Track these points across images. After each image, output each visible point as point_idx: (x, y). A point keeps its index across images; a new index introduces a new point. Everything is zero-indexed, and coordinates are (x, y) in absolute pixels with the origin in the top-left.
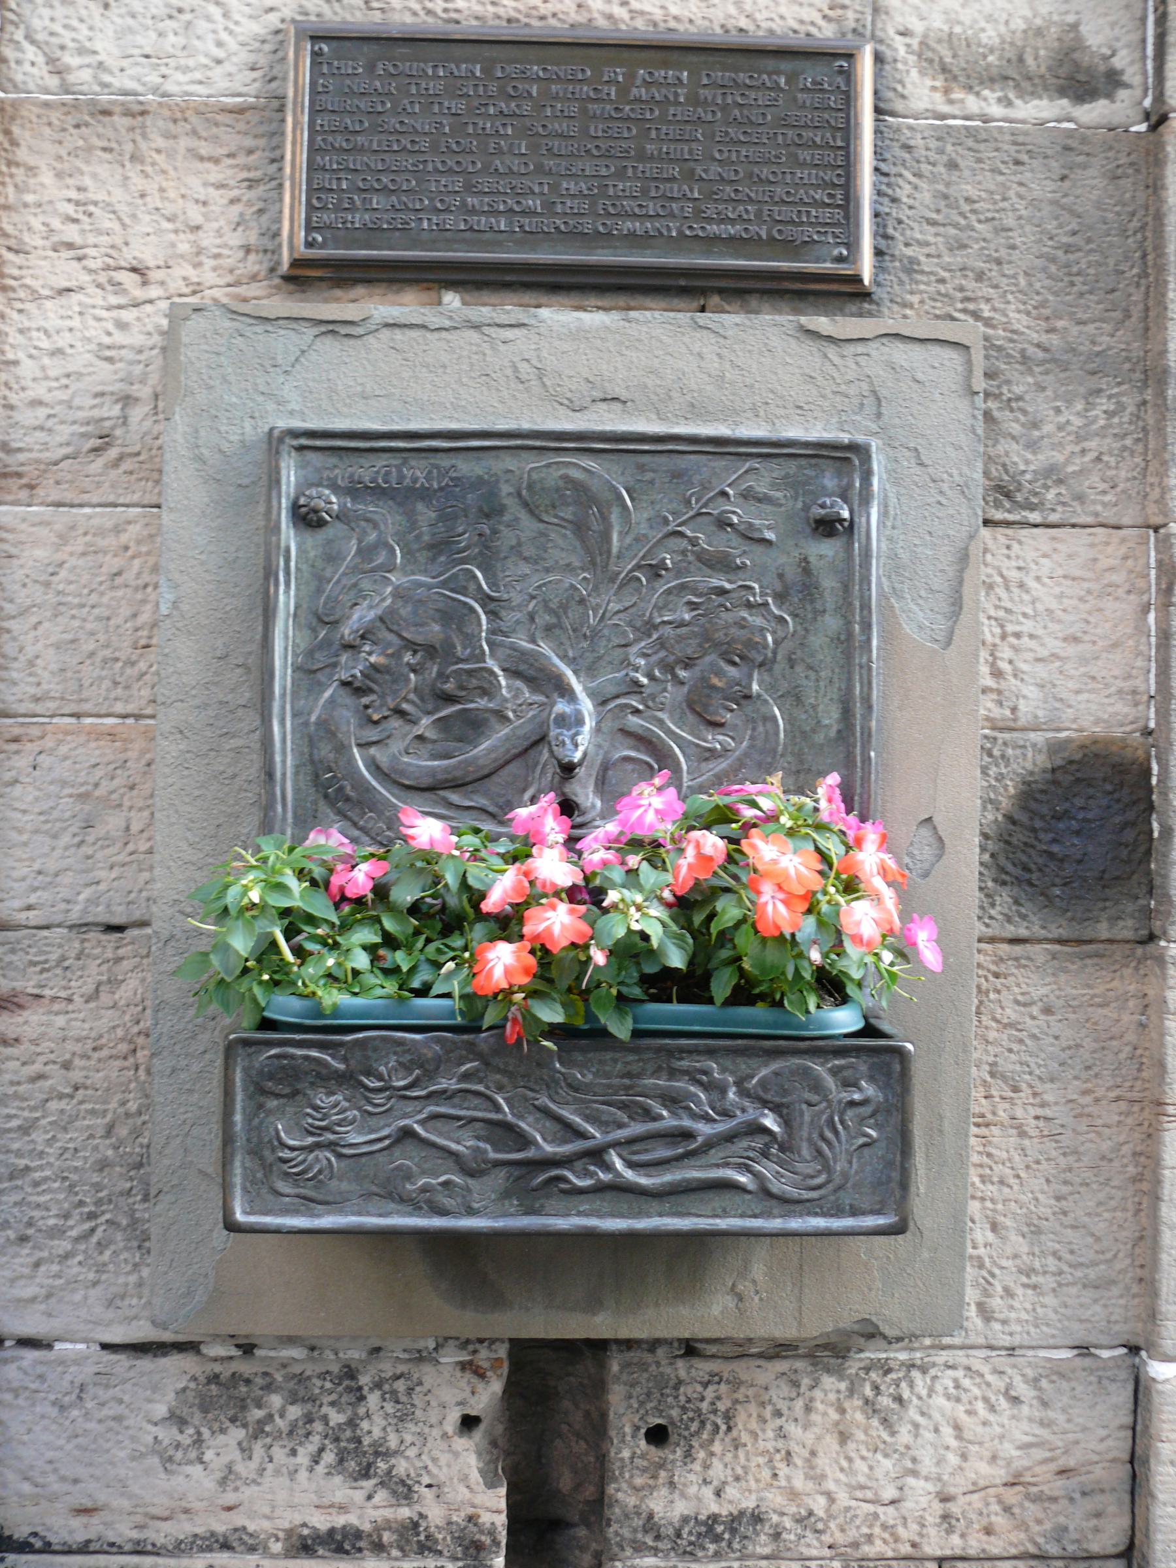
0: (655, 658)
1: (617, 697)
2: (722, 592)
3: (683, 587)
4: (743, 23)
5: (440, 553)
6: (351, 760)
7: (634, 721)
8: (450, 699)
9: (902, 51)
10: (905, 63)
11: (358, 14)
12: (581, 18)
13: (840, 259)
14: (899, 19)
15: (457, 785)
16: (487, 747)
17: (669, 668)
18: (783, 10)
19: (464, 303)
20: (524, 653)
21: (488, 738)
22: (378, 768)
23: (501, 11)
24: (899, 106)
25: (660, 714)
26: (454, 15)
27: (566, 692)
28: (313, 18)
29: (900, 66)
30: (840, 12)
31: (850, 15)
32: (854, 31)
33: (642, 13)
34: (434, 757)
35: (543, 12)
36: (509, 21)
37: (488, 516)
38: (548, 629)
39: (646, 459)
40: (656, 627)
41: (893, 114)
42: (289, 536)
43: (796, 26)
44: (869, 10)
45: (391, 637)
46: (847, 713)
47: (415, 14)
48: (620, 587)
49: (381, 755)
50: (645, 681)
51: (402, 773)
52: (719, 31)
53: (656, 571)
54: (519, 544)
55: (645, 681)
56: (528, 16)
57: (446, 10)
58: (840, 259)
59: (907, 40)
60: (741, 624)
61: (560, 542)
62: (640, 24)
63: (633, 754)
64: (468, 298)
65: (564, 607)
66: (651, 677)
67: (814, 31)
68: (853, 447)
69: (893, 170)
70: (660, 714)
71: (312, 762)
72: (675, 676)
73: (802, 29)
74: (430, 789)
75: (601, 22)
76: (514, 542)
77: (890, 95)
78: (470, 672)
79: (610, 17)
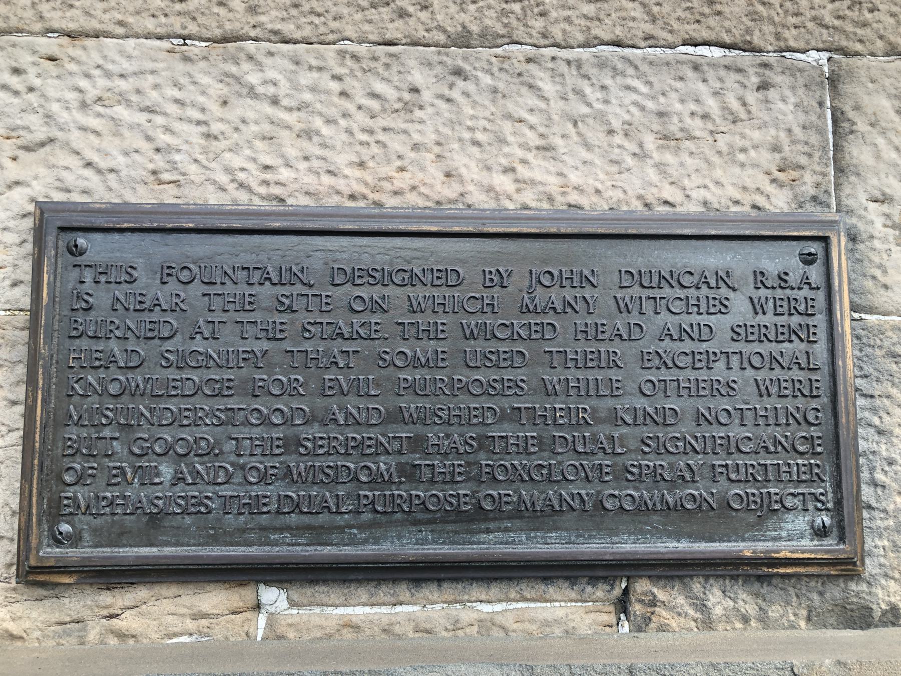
4: (670, 193)
9: (879, 222)
10: (885, 240)
11: (141, 189)
12: (449, 191)
13: (821, 533)
14: (874, 181)
18: (718, 173)
19: (293, 604)
23: (341, 184)
24: (881, 298)
26: (276, 191)
28: (76, 198)
29: (877, 244)
30: (794, 174)
31: (809, 178)
32: (814, 199)
33: (533, 183)
35: (398, 184)
36: (352, 197)
41: (871, 310)
43: (737, 195)
44: (831, 170)
47: (222, 189)
52: (637, 205)
56: (376, 189)
57: (266, 183)
58: (821, 533)
59: (885, 208)
62: (529, 197)
64: (296, 595)
67: (761, 201)
69: (877, 389)
73: (747, 199)
75: (480, 200)
77: (869, 284)
79: (490, 189)
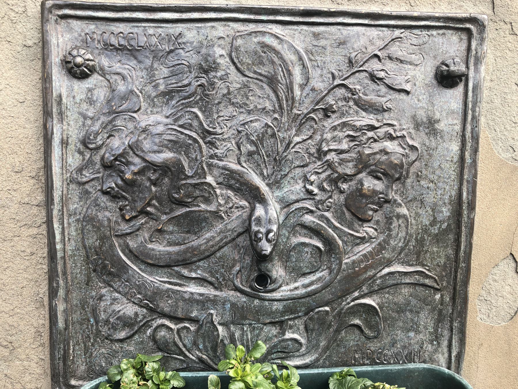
0: (323, 176)
1: (297, 201)
2: (372, 128)
3: (344, 125)
5: (172, 98)
6: (112, 246)
7: (308, 218)
8: (181, 203)
15: (186, 263)
16: (209, 235)
17: (334, 181)
20: (232, 171)
21: (209, 230)
22: (131, 251)
25: (326, 214)
27: (261, 199)
34: (170, 244)
37: (206, 72)
38: (250, 154)
39: (322, 28)
40: (326, 153)
42: (61, 83)
45: (137, 160)
46: (457, 213)
48: (301, 125)
49: (132, 244)
50: (316, 191)
51: (148, 255)
53: (327, 112)
54: (229, 93)
55: (316, 191)
60: (384, 152)
61: (259, 92)
63: (307, 240)
65: (261, 139)
66: (322, 189)
68: (473, 20)
70: (326, 214)
71: (85, 247)
72: (338, 187)
74: (168, 266)
76: (225, 91)
78: (195, 186)
